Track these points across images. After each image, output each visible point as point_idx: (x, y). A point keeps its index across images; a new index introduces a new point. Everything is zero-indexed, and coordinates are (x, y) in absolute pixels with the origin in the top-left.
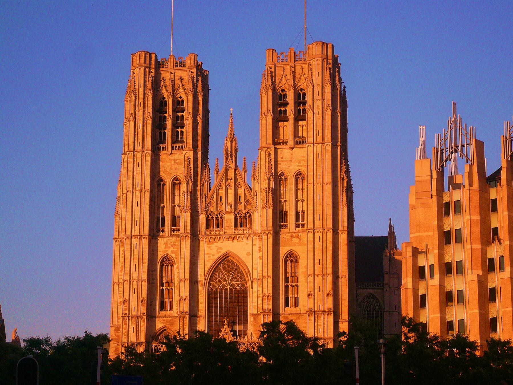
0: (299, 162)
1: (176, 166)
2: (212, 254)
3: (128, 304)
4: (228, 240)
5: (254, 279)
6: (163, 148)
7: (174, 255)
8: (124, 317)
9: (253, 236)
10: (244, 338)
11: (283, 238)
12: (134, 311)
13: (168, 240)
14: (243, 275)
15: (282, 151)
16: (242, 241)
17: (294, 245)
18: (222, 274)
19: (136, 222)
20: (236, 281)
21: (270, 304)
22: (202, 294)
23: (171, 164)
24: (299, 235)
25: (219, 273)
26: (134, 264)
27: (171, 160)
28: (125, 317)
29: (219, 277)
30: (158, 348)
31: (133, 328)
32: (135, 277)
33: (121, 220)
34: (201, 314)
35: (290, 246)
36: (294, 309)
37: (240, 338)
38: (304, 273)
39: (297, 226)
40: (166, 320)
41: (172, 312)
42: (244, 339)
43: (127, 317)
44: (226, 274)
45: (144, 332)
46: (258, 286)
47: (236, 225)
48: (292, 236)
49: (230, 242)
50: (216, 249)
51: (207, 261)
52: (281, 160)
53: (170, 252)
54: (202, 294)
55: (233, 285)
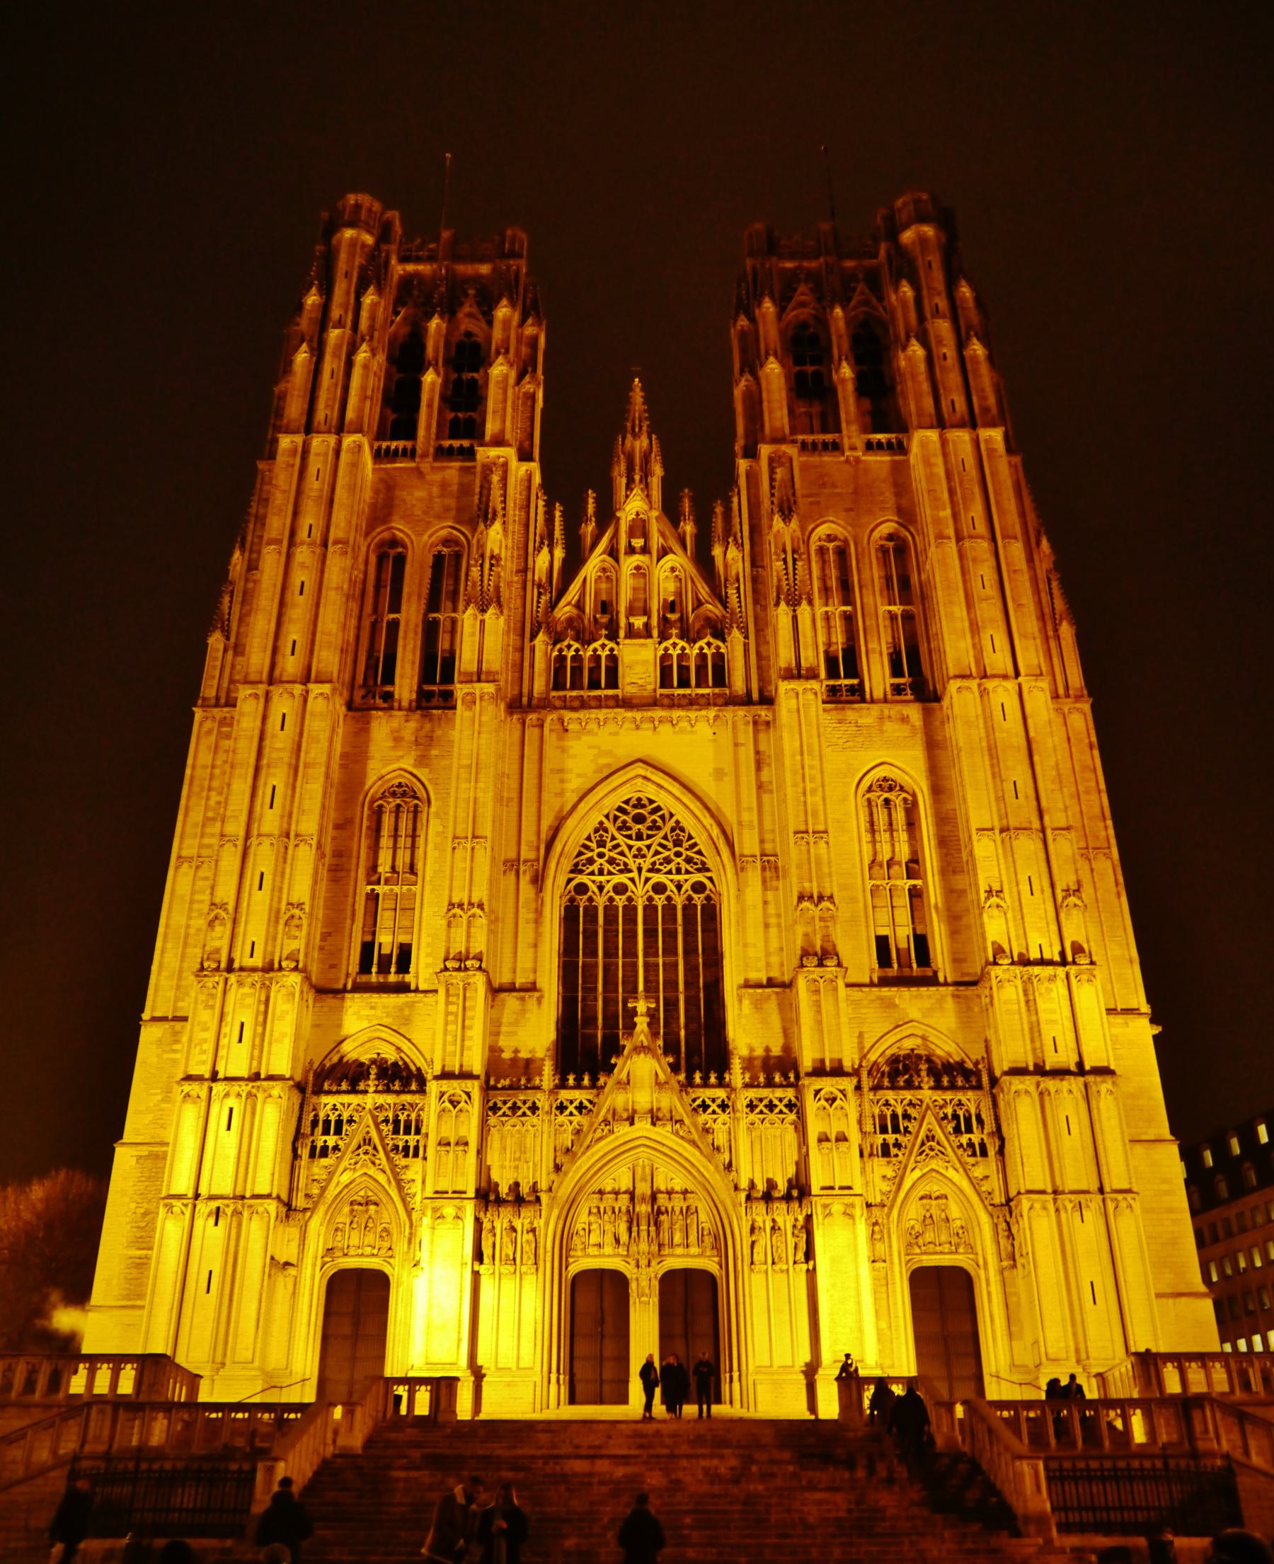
3: (229, 926)
4: (637, 727)
12: (252, 956)
14: (699, 853)
16: (692, 732)
20: (670, 872)
25: (601, 844)
29: (601, 855)
30: (340, 1115)
31: (242, 1024)
33: (230, 653)
39: (897, 689)
40: (384, 1007)
44: (630, 847)
47: (665, 681)
48: (881, 718)
53: (412, 761)
55: (660, 888)
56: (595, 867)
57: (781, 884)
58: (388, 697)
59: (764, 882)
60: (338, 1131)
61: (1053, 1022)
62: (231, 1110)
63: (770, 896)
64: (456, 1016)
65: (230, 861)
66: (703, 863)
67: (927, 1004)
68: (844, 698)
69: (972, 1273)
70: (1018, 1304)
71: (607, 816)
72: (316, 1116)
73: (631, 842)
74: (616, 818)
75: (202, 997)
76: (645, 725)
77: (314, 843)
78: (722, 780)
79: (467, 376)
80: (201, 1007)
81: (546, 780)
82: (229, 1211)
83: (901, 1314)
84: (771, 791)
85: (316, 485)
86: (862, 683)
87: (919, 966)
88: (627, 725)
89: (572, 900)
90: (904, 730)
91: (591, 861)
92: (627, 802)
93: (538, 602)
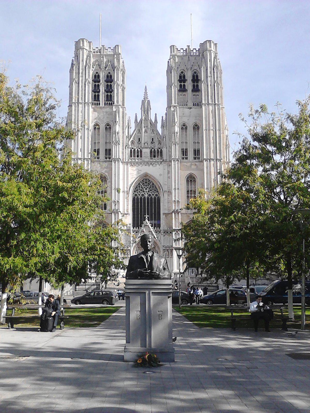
0: (196, 117)
6: (98, 103)
10: (159, 228)
14: (157, 189)
15: (183, 109)
17: (193, 170)
18: (141, 188)
25: (139, 187)
29: (139, 189)
35: (190, 171)
39: (195, 158)
41: (106, 210)
44: (144, 188)
46: (168, 195)
51: (131, 178)
55: (150, 195)
56: (138, 191)
63: (169, 197)
66: (157, 191)
71: (140, 182)
73: (145, 187)
74: (142, 182)
79: (109, 84)
81: (129, 175)
88: (144, 165)
91: (138, 190)
92: (144, 179)
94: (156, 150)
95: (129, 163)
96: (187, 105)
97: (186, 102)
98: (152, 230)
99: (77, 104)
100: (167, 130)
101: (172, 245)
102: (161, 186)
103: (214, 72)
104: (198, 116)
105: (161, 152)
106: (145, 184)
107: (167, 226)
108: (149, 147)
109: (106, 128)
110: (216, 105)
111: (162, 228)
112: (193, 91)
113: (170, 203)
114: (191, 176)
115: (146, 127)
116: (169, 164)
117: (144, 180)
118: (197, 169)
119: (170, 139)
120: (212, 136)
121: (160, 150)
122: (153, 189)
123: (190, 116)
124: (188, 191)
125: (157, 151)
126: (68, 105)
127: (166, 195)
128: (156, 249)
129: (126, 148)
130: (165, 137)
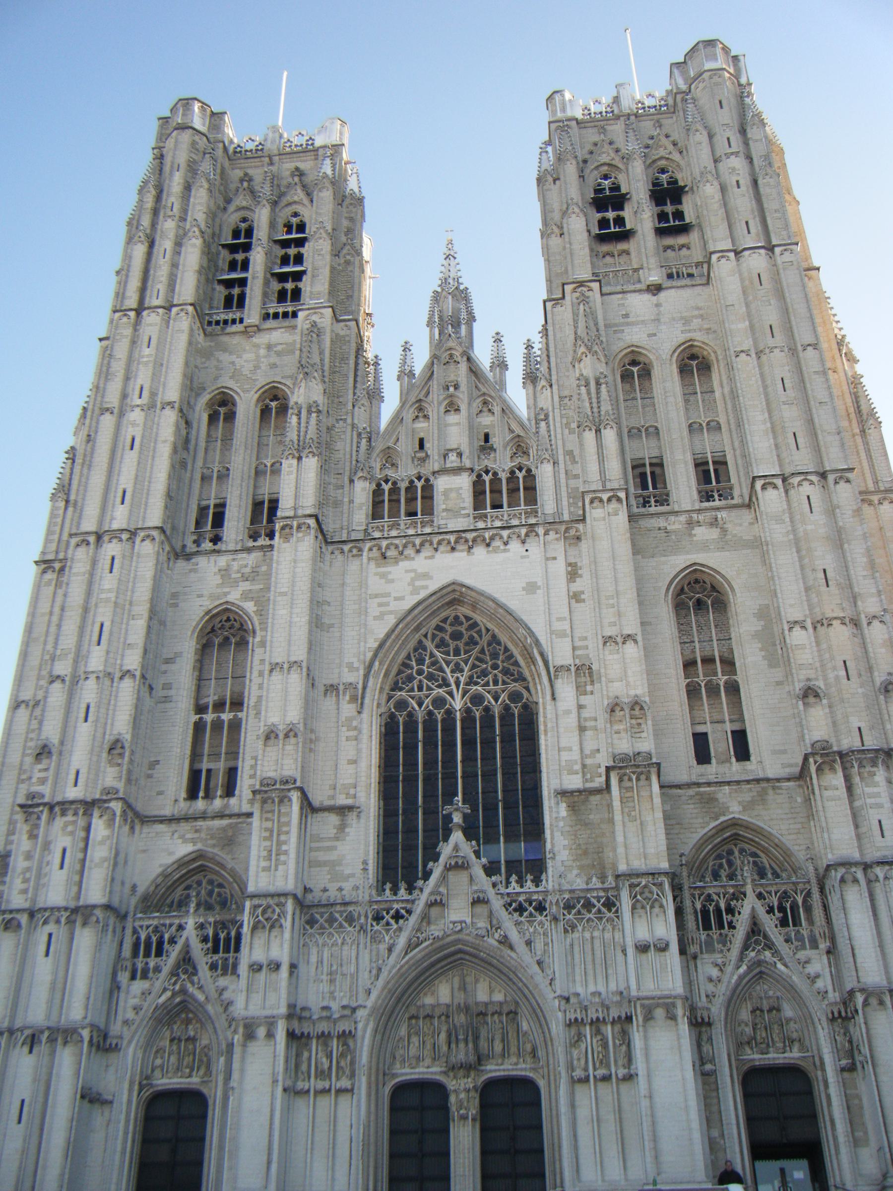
0: (686, 321)
1: (274, 359)
2: (394, 595)
4: (453, 549)
5: (558, 669)
7: (252, 603)
8: (31, 810)
9: (546, 533)
10: (537, 881)
11: (660, 529)
13: (234, 560)
14: (516, 664)
16: (505, 551)
17: (705, 547)
19: (120, 494)
21: (644, 735)
22: (355, 728)
23: (258, 356)
24: (716, 519)
25: (420, 661)
26: (99, 620)
27: (257, 346)
28: (36, 810)
29: (420, 672)
30: (162, 937)
31: (64, 851)
32: (96, 660)
34: (349, 802)
35: (688, 553)
36: (734, 769)
37: (521, 882)
38: (757, 635)
39: (707, 496)
40: (208, 829)
41: (233, 801)
42: (537, 886)
43: (41, 808)
44: (448, 663)
45: (106, 864)
46: (581, 690)
48: (690, 524)
49: (461, 556)
50: (409, 580)
52: (622, 320)
53: (239, 597)
54: (355, 728)
55: (477, 699)
56: (415, 683)
57: (597, 686)
58: (216, 540)
59: (577, 688)
60: (159, 953)
61: (879, 806)
62: (50, 935)
63: (584, 700)
64: (272, 831)
65: (57, 695)
66: (520, 674)
67: (747, 797)
68: (653, 509)
69: (812, 1075)
70: (861, 1108)
71: (426, 636)
72: (138, 938)
74: (434, 636)
75: (26, 828)
76: (459, 547)
77: (138, 674)
78: (535, 593)
80: (25, 837)
82: (44, 1037)
83: (734, 1122)
84: (584, 601)
85: (147, 351)
86: (668, 495)
87: (738, 760)
88: (442, 548)
89: (392, 716)
90: (714, 534)
91: (410, 679)
92: (445, 620)
93: (358, 443)
94: (503, 476)
95: (368, 545)
96: (639, 281)
97: (636, 270)
98: (491, 893)
99: (132, 314)
100: (555, 387)
101: (622, 987)
102: (537, 642)
103: (746, 143)
104: (701, 316)
105: (531, 489)
106: (452, 645)
107: (581, 868)
108: (467, 463)
109: (265, 412)
110: (777, 250)
111: (550, 881)
112: (661, 232)
113: (595, 729)
114: (697, 581)
115: (452, 389)
116: (572, 532)
117: (447, 627)
118: (725, 542)
119: (568, 425)
120: (779, 373)
121: (520, 475)
122: (495, 667)
123: (657, 320)
124: (689, 665)
125: (509, 480)
126: (103, 335)
127: (566, 689)
128: (525, 1026)
129: (352, 481)
130: (547, 416)
